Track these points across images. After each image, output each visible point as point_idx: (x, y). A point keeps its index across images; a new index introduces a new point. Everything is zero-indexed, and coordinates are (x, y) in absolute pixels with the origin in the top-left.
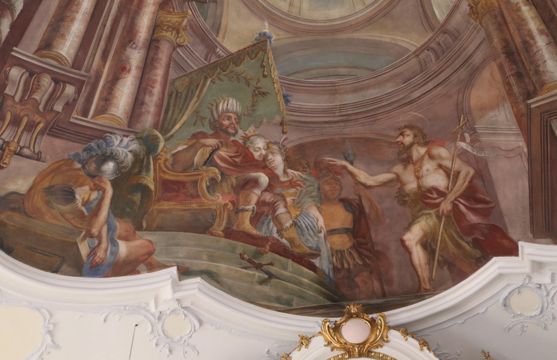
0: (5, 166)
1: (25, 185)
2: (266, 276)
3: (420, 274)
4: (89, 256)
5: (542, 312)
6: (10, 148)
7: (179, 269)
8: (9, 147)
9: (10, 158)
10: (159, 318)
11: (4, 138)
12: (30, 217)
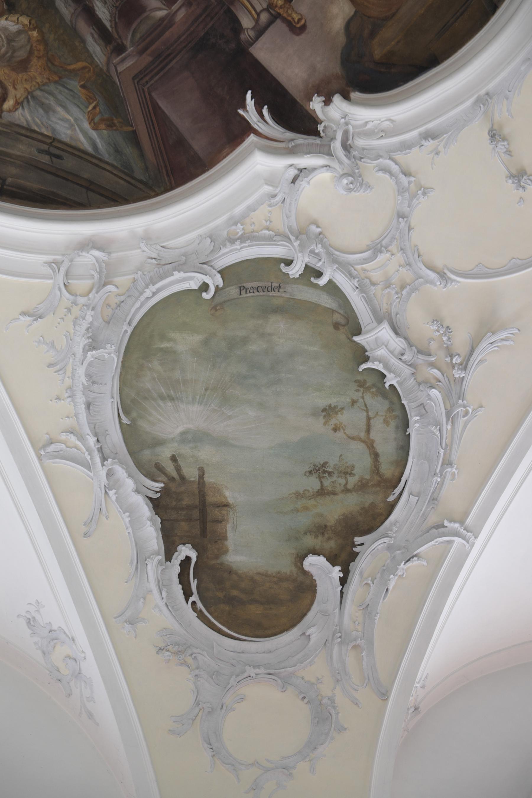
0: (303, 22)
1: (342, 5)
6: (279, 5)
8: (276, 6)
9: (293, 10)
11: (261, 8)
12: (394, 15)
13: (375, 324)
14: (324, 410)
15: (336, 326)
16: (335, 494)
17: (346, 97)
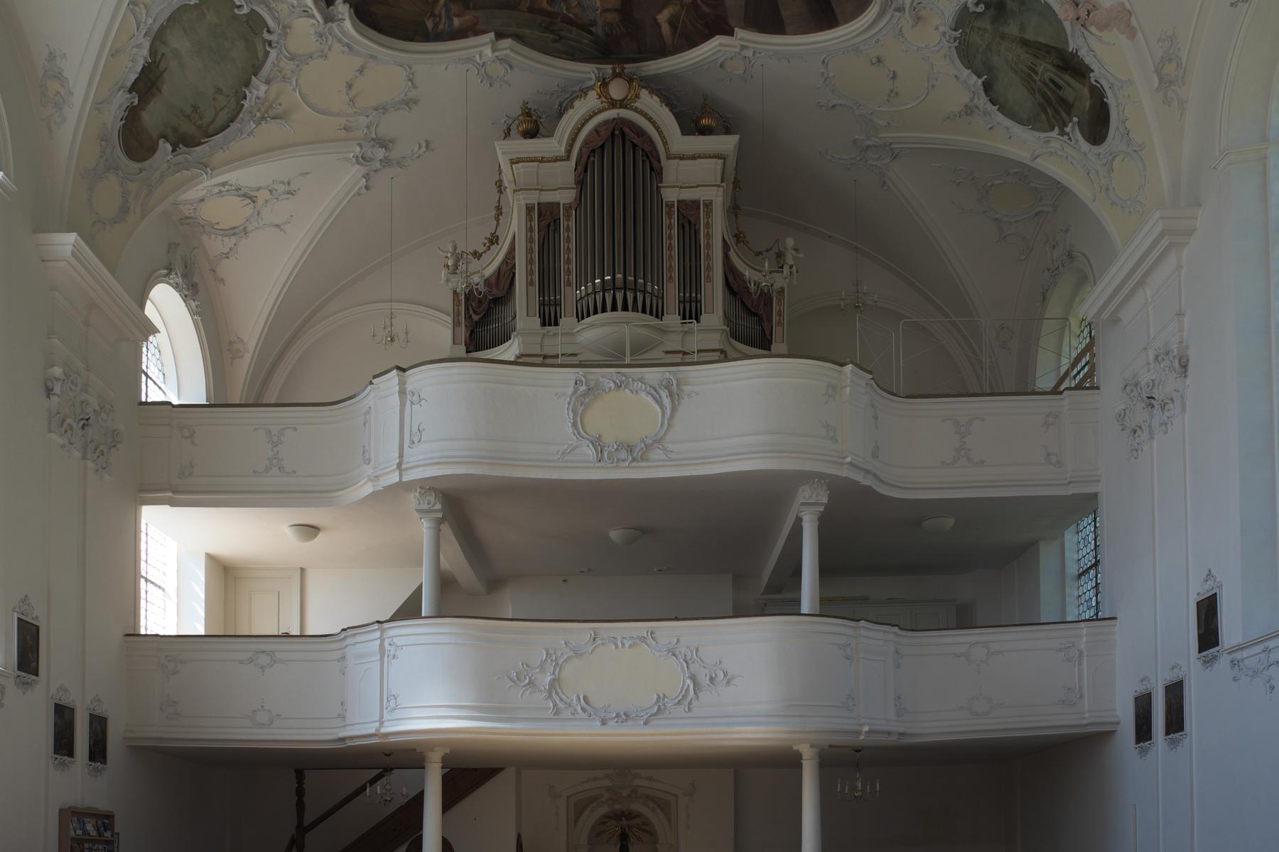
2: (558, 38)
3: (666, 40)
4: (433, 29)
5: (745, 72)
7: (495, 34)
10: (483, 66)
13: (264, 81)
14: (218, 89)
15: (253, 66)
16: (191, 121)
17: (351, 7)
